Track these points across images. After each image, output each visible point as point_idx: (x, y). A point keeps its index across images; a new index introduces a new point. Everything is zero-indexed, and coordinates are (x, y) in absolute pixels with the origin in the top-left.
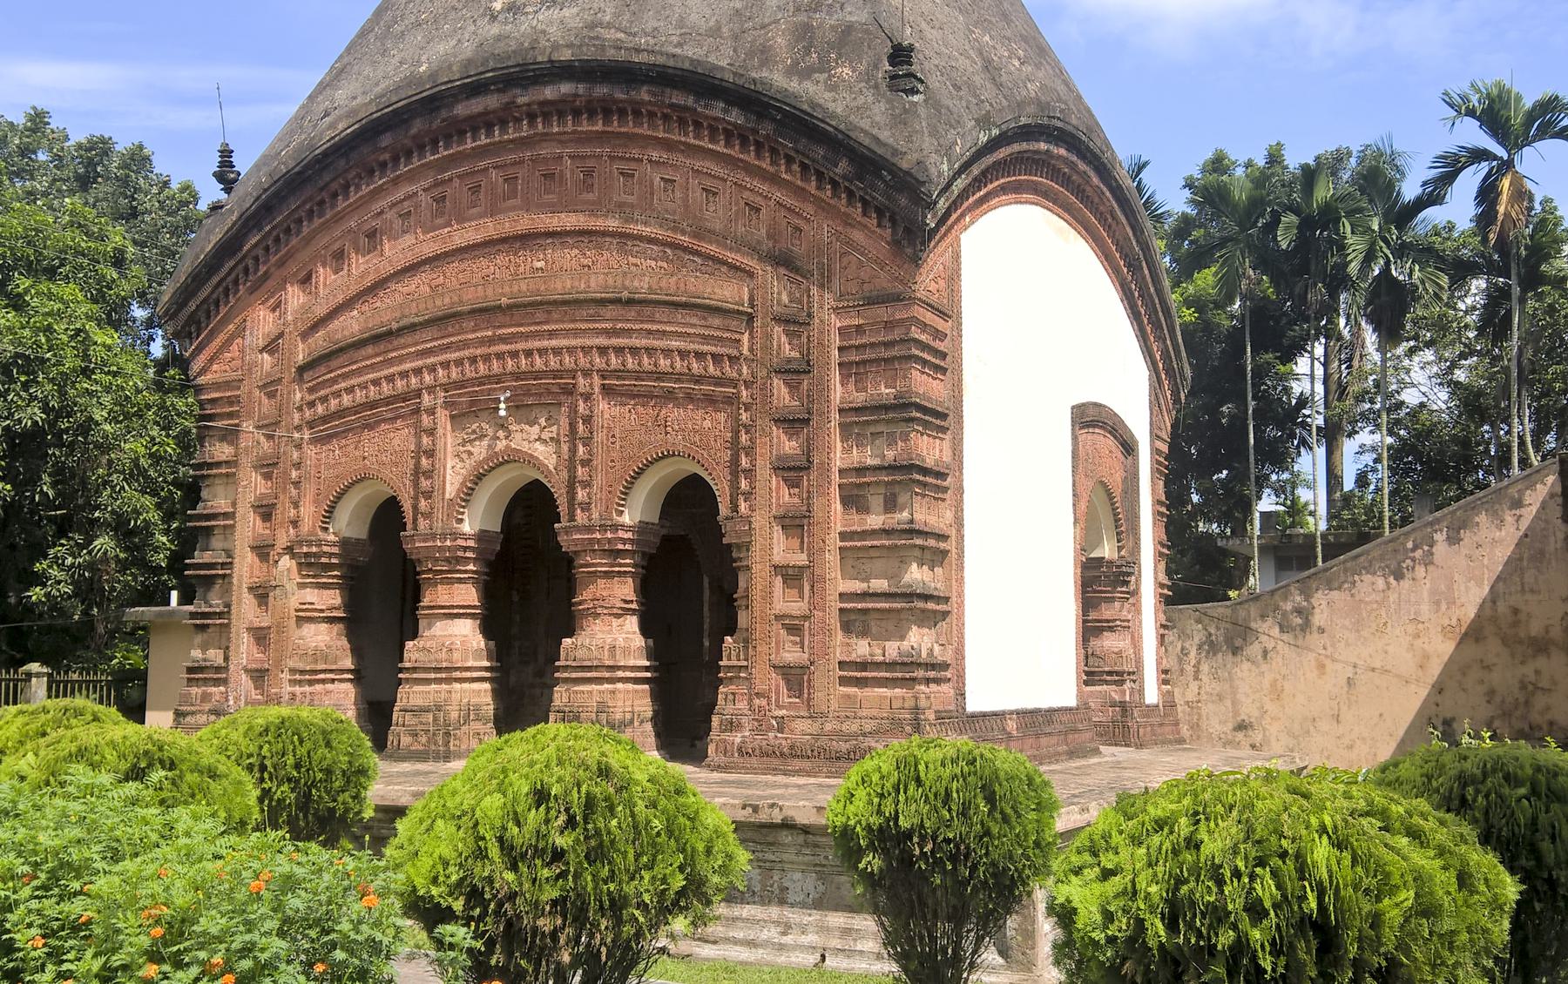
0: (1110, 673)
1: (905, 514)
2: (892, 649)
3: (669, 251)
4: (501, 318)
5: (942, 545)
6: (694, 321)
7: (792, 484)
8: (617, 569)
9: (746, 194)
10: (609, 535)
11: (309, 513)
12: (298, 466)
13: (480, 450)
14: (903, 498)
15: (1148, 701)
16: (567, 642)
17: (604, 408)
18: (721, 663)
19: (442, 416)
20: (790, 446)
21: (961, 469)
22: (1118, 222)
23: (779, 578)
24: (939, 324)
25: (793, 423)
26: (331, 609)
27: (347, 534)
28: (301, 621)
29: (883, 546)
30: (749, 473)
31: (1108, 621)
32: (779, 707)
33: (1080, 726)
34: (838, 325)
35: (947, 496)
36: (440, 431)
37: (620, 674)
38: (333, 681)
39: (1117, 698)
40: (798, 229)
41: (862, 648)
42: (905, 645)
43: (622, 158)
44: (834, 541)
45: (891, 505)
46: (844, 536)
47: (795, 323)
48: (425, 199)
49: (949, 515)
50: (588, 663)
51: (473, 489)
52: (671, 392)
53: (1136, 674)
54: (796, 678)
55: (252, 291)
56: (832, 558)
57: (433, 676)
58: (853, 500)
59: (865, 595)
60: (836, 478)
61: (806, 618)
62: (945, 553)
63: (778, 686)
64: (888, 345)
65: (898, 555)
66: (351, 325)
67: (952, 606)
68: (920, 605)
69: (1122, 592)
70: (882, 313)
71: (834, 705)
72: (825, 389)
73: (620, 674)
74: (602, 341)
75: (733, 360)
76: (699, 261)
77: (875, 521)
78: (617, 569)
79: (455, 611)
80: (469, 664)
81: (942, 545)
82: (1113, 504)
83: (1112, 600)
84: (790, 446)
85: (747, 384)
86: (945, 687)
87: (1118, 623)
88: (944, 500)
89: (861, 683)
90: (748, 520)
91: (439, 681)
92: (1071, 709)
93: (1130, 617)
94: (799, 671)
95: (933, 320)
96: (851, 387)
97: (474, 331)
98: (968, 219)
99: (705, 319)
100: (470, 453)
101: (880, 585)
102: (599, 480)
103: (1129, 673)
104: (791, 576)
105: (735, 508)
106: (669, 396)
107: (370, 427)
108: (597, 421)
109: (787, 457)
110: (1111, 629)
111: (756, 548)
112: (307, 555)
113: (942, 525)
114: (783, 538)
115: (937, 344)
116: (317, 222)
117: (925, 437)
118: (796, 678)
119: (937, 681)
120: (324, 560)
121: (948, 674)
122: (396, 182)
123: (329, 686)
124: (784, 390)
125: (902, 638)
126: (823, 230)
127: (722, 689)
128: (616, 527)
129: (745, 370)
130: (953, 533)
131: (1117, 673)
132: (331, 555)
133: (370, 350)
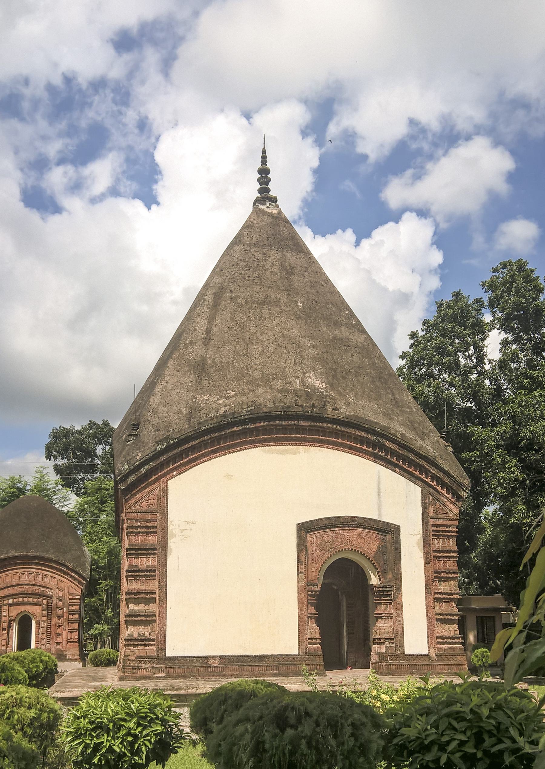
0: (378, 639)
5: (154, 596)
15: (409, 650)
24: (149, 517)
31: (380, 614)
62: (155, 598)
69: (385, 600)
81: (154, 596)
83: (380, 604)
86: (150, 648)
87: (383, 615)
88: (155, 579)
95: (144, 517)
98: (175, 473)
103: (387, 639)
110: (381, 618)
115: (151, 524)
119: (146, 645)
130: (157, 592)
131: (380, 639)
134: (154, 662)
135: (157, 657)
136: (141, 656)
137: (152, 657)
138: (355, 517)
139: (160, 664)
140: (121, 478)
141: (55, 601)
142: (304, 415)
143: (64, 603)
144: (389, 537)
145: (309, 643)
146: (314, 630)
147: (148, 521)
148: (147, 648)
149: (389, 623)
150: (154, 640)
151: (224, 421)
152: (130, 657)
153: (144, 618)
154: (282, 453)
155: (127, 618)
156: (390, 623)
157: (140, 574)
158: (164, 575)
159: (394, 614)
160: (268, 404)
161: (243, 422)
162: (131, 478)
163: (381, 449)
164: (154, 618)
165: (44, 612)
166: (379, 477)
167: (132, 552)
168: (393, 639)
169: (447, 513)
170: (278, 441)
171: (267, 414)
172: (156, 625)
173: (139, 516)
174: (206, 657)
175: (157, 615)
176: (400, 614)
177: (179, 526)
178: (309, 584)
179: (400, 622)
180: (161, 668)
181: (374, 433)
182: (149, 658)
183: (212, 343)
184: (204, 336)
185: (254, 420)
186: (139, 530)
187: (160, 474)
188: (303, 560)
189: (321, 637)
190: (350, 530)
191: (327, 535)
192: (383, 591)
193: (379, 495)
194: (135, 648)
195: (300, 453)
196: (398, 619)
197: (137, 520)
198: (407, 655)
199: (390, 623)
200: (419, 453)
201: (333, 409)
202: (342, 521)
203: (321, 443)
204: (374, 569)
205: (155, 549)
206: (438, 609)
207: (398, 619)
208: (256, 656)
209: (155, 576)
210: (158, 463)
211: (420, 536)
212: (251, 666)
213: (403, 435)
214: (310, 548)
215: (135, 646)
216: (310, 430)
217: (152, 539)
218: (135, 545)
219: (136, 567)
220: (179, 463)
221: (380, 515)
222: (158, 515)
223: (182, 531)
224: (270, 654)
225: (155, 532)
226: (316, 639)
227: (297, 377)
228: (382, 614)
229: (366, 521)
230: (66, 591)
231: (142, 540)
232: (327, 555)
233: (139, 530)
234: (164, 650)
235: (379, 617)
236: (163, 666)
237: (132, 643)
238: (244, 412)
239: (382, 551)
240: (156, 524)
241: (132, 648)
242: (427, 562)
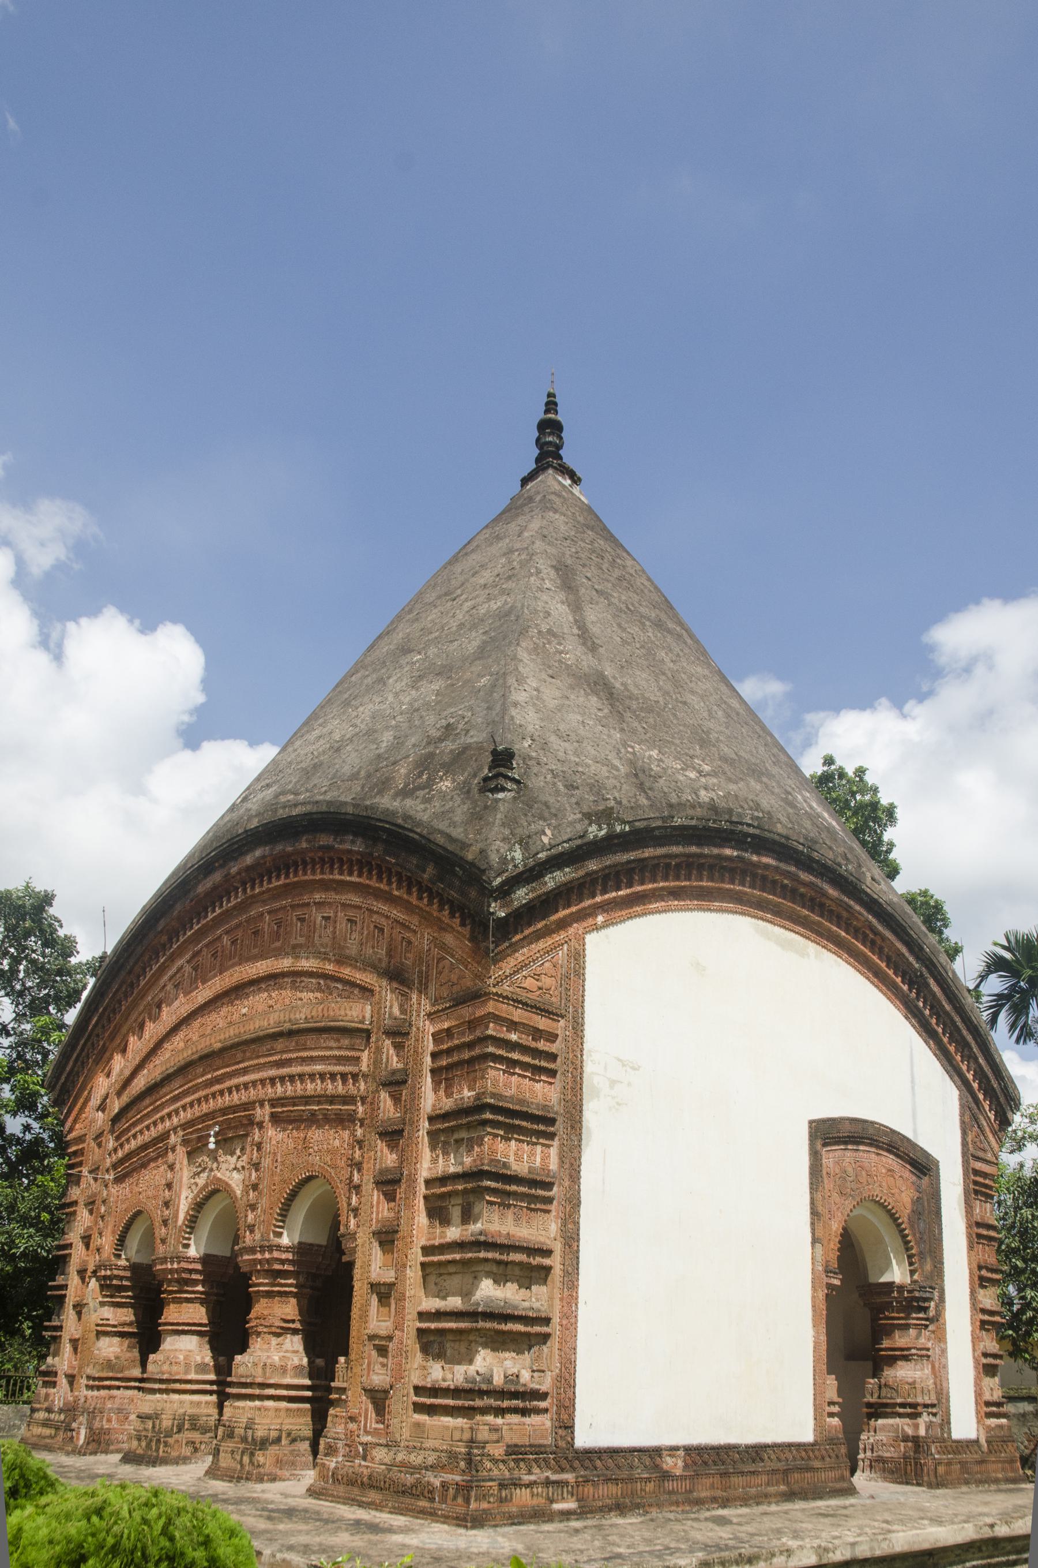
0: (903, 1405)
1: (479, 1225)
2: (458, 1375)
3: (322, 982)
4: (218, 1062)
6: (333, 1044)
7: (390, 1197)
8: (276, 1289)
9: (375, 916)
10: (267, 1255)
11: (107, 1242)
12: (104, 1202)
13: (201, 1181)
14: (476, 1210)
16: (238, 1358)
17: (273, 1134)
18: (333, 1384)
19: (181, 1151)
20: (390, 1159)
21: (575, 1176)
22: (884, 938)
23: (375, 1296)
24: (542, 1023)
25: (393, 1135)
26: (124, 1324)
27: (136, 1259)
28: (99, 1334)
29: (453, 1262)
30: (357, 1188)
32: (367, 1433)
33: (817, 1464)
34: (432, 1030)
35: (553, 1207)
36: (177, 1166)
37: (271, 1392)
38: (118, 1388)
39: (910, 1432)
40: (409, 943)
41: (437, 1373)
42: (472, 1369)
43: (298, 905)
44: (417, 1256)
45: (467, 1217)
46: (427, 1250)
47: (399, 1034)
49: (554, 1228)
50: (243, 1380)
51: (197, 1217)
52: (313, 1114)
54: (379, 1398)
56: (413, 1275)
57: (157, 1386)
58: (437, 1212)
59: (439, 1315)
60: (422, 1189)
61: (390, 1338)
62: (548, 1269)
63: (367, 1410)
64: (470, 1045)
65: (471, 1270)
67: (555, 1328)
68: (488, 1325)
69: (918, 1319)
70: (466, 1012)
71: (406, 1433)
72: (415, 1096)
73: (271, 1392)
74: (273, 1072)
75: (355, 1076)
76: (340, 986)
77: (454, 1233)
78: (276, 1289)
79: (180, 1328)
80: (189, 1377)
81: (546, 1262)
82: (899, 1225)
83: (907, 1327)
84: (390, 1159)
85: (363, 1100)
86: (534, 1419)
87: (913, 1351)
89: (431, 1410)
90: (353, 1236)
91: (161, 1391)
92: (799, 1446)
93: (929, 1345)
94: (382, 1395)
96: (442, 1093)
97: (203, 1076)
99: (338, 1040)
100: (196, 1184)
101: (455, 1302)
102: (264, 1202)
104: (384, 1292)
105: (347, 1226)
106: (313, 1120)
107: (144, 1166)
108: (267, 1147)
109: (387, 1170)
110: (906, 1358)
111: (358, 1264)
112: (105, 1277)
113: (542, 1239)
114: (379, 1253)
115: (542, 1045)
116: (130, 999)
117: (513, 1142)
118: (379, 1398)
119: (524, 1412)
120: (115, 1282)
121: (543, 1404)
123: (115, 1392)
124: (389, 1102)
125: (471, 1362)
126: (424, 938)
127: (331, 1411)
128: (271, 1248)
129: (362, 1086)
130: (558, 1247)
131: (913, 1406)
132: (121, 1278)
135: (556, 1450)
136: (516, 1446)
137: (543, 1449)
138: (887, 1127)
139: (562, 1470)
140: (503, 884)
144: (926, 1180)
146: (832, 1381)
147: (537, 1034)
148: (527, 1420)
149: (922, 1370)
150: (543, 1396)
151: (714, 821)
153: (520, 1327)
155: (424, 1325)
157: (514, 1188)
158: (574, 1202)
162: (522, 895)
164: (544, 1329)
167: (501, 1118)
169: (984, 1151)
173: (518, 1015)
175: (556, 1320)
177: (605, 1068)
180: (566, 1483)
186: (515, 1056)
187: (574, 909)
188: (820, 1209)
189: (840, 1400)
190: (878, 1154)
192: (918, 1299)
193: (913, 1088)
194: (499, 1421)
197: (513, 1026)
202: (871, 1131)
204: (902, 1249)
208: (747, 1447)
209: (549, 1200)
210: (581, 873)
212: (742, 1473)
215: (500, 1412)
219: (505, 1165)
220: (614, 894)
221: (915, 1131)
223: (613, 1083)
224: (768, 1439)
225: (552, 1073)
228: (909, 1349)
229: (902, 1140)
235: (904, 1356)
236: (569, 1477)
237: (492, 1402)
240: (553, 1048)
241: (490, 1418)
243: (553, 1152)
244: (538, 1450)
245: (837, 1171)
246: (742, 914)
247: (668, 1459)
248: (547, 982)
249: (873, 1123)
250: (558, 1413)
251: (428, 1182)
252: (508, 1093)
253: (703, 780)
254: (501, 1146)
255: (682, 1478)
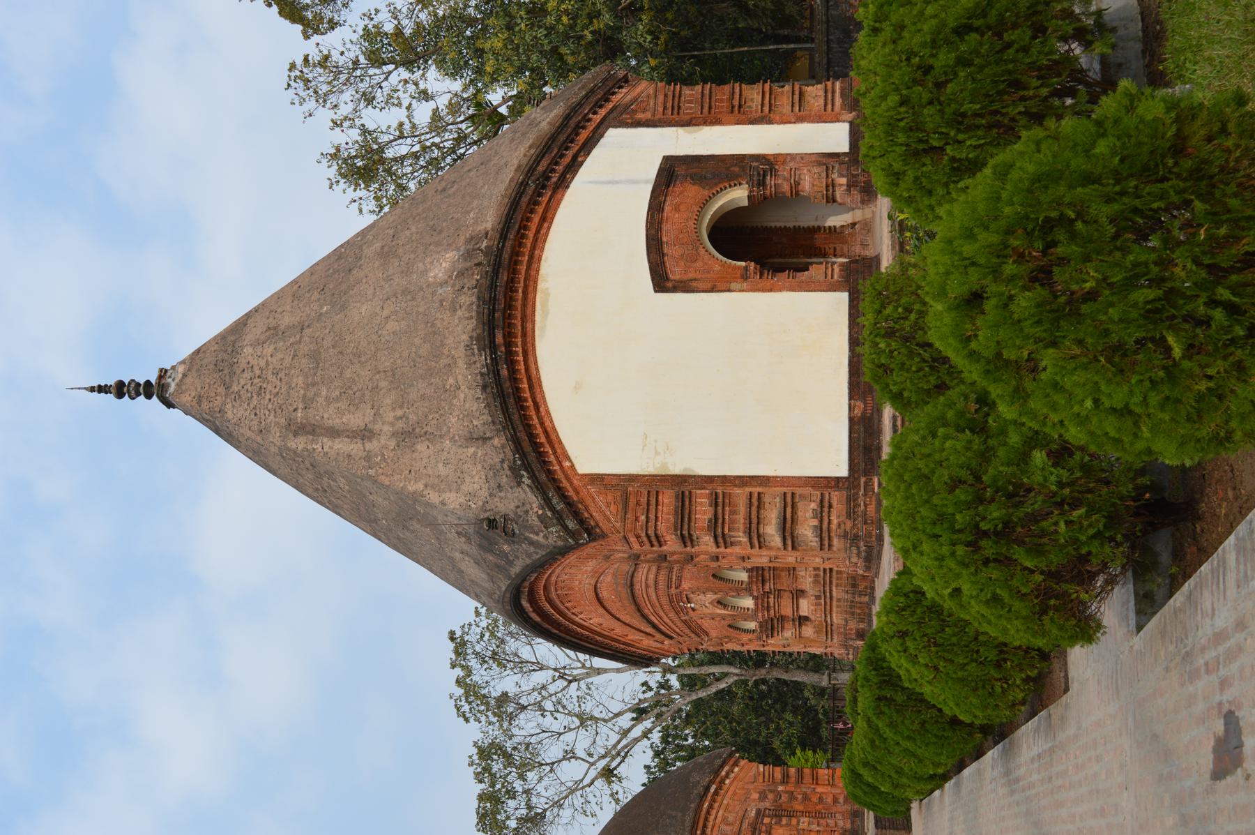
0: (827, 190)
15: (843, 146)
39: (845, 187)
48: (581, 616)
49: (738, 491)
53: (827, 160)
55: (633, 646)
60: (722, 549)
66: (650, 630)
67: (788, 490)
86: (834, 501)
87: (792, 181)
98: (567, 464)
119: (830, 507)
122: (574, 622)
130: (748, 490)
131: (827, 186)
133: (662, 627)
134: (857, 494)
139: (859, 484)
140: (571, 537)
141: (767, 804)
142: (492, 279)
143: (771, 791)
144: (680, 171)
145: (832, 278)
151: (492, 388)
152: (848, 529)
154: (546, 314)
156: (805, 171)
158: (724, 479)
159: (792, 165)
160: (470, 327)
161: (495, 362)
162: (571, 524)
163: (548, 178)
165: (784, 821)
166: (590, 182)
168: (827, 169)
170: (528, 317)
171: (486, 328)
172: (798, 491)
174: (851, 420)
175: (785, 490)
176: (792, 157)
178: (745, 276)
179: (803, 156)
180: (865, 483)
181: (523, 185)
182: (851, 500)
183: (370, 426)
184: (359, 440)
185: (493, 347)
186: (652, 516)
191: (672, 252)
193: (617, 182)
195: (547, 289)
196: (798, 159)
198: (850, 149)
199: (805, 171)
200: (559, 127)
201: (486, 237)
203: (534, 260)
205: (683, 492)
206: (786, 109)
207: (798, 159)
209: (724, 493)
211: (680, 130)
213: (530, 147)
214: (690, 276)
215: (829, 523)
216: (513, 271)
217: (668, 499)
218: (676, 523)
219: (710, 521)
221: (647, 182)
222: (630, 489)
223: (657, 453)
225: (657, 492)
226: (826, 268)
227: (434, 293)
230: (751, 786)
231: (668, 514)
232: (702, 252)
233: (652, 516)
234: (838, 479)
236: (863, 480)
238: (482, 360)
239: (699, 180)
242: (718, 122)
243: (698, 492)
244: (849, 499)
245: (682, 264)
246: (534, 349)
247: (856, 412)
248: (610, 498)
249: (647, 230)
250: (831, 488)
251: (718, 547)
252: (672, 520)
253: (462, 387)
254: (699, 524)
255: (865, 404)
